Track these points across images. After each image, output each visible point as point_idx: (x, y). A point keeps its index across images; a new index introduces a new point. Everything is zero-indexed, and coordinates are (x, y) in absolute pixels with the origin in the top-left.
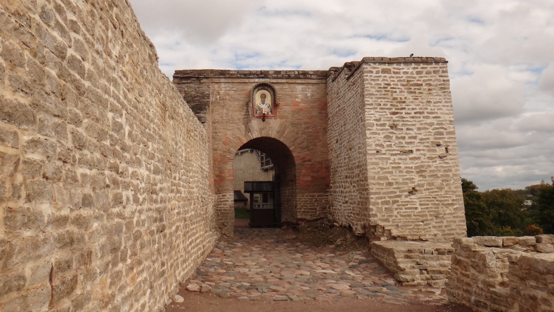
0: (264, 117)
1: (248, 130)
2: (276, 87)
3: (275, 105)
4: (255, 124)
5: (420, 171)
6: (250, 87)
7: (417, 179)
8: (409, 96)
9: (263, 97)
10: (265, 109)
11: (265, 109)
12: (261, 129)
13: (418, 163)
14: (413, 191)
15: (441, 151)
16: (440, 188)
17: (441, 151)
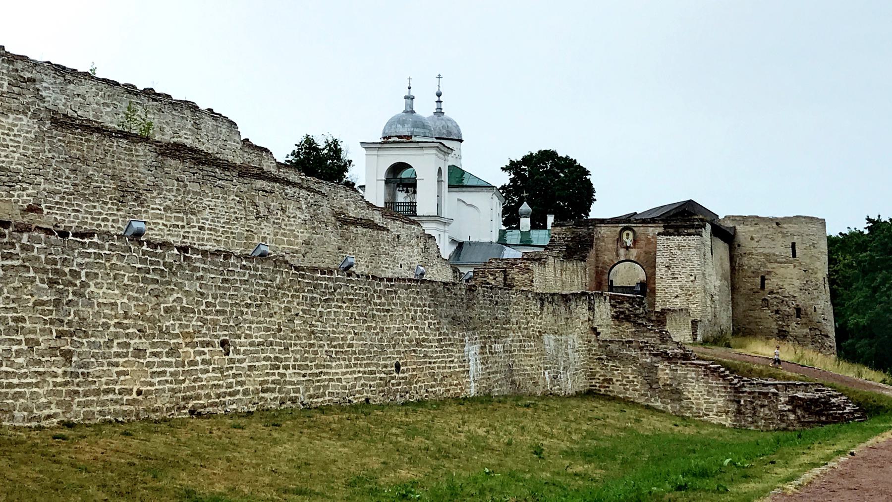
0: (627, 248)
1: (618, 255)
2: (635, 229)
3: (635, 241)
4: (622, 251)
5: (681, 288)
6: (619, 229)
7: (679, 291)
8: (679, 252)
9: (628, 235)
10: (629, 243)
11: (629, 243)
12: (626, 255)
13: (680, 284)
14: (677, 297)
15: (692, 278)
16: (691, 295)
17: (692, 278)
